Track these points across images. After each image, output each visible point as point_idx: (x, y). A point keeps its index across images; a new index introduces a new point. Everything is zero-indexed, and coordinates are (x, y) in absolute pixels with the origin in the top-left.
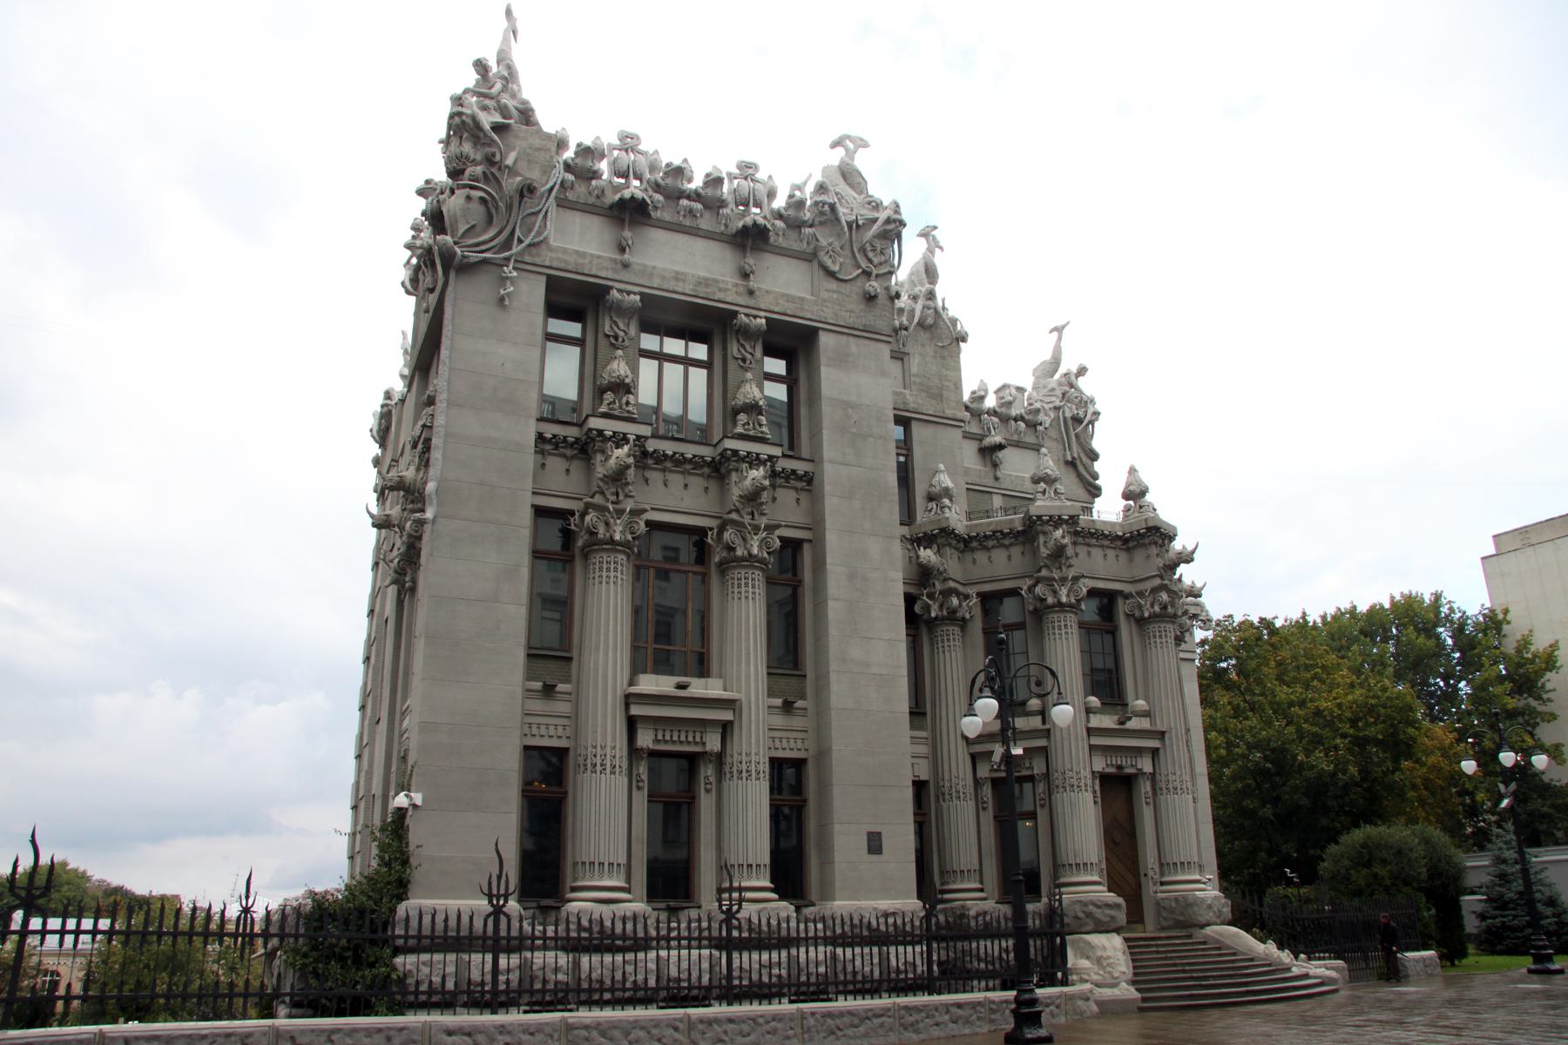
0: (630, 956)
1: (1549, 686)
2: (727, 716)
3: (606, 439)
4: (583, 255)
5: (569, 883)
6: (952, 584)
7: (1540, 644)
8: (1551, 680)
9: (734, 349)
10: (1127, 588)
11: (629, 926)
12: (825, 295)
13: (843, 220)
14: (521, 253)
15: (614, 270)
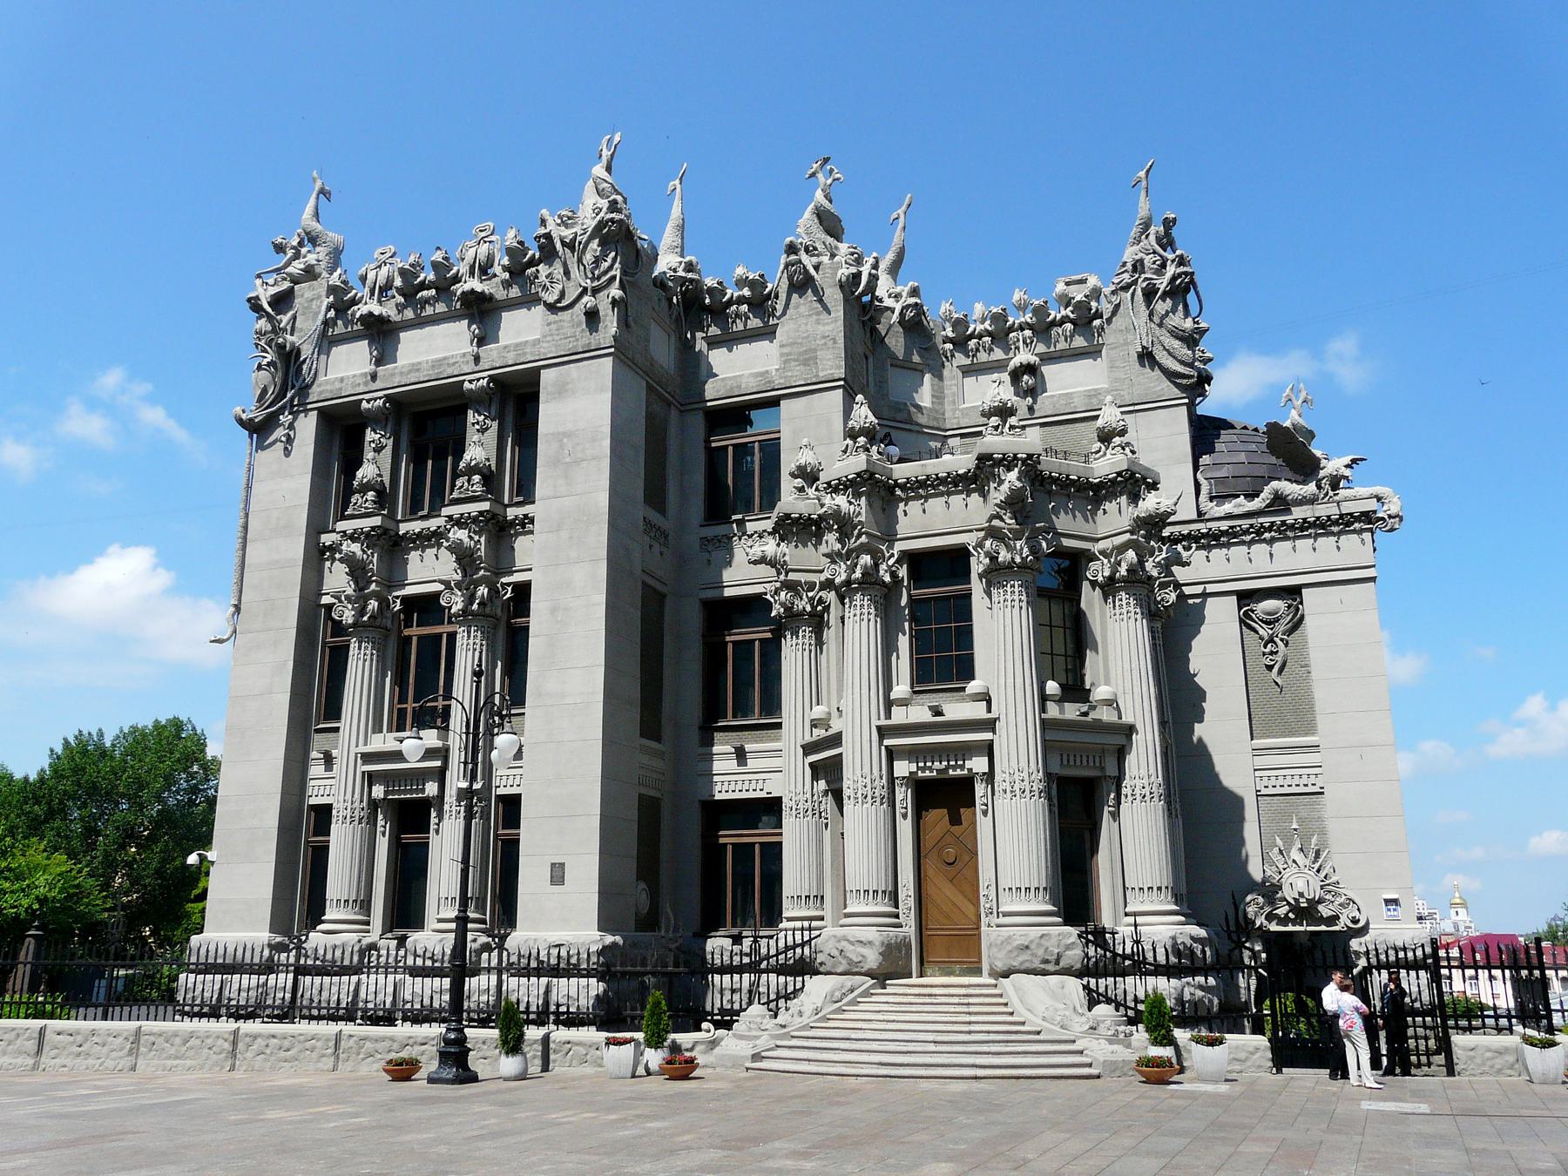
0: (336, 979)
2: (438, 763)
4: (342, 380)
6: (792, 576)
11: (338, 953)
13: (558, 246)
15: (366, 384)
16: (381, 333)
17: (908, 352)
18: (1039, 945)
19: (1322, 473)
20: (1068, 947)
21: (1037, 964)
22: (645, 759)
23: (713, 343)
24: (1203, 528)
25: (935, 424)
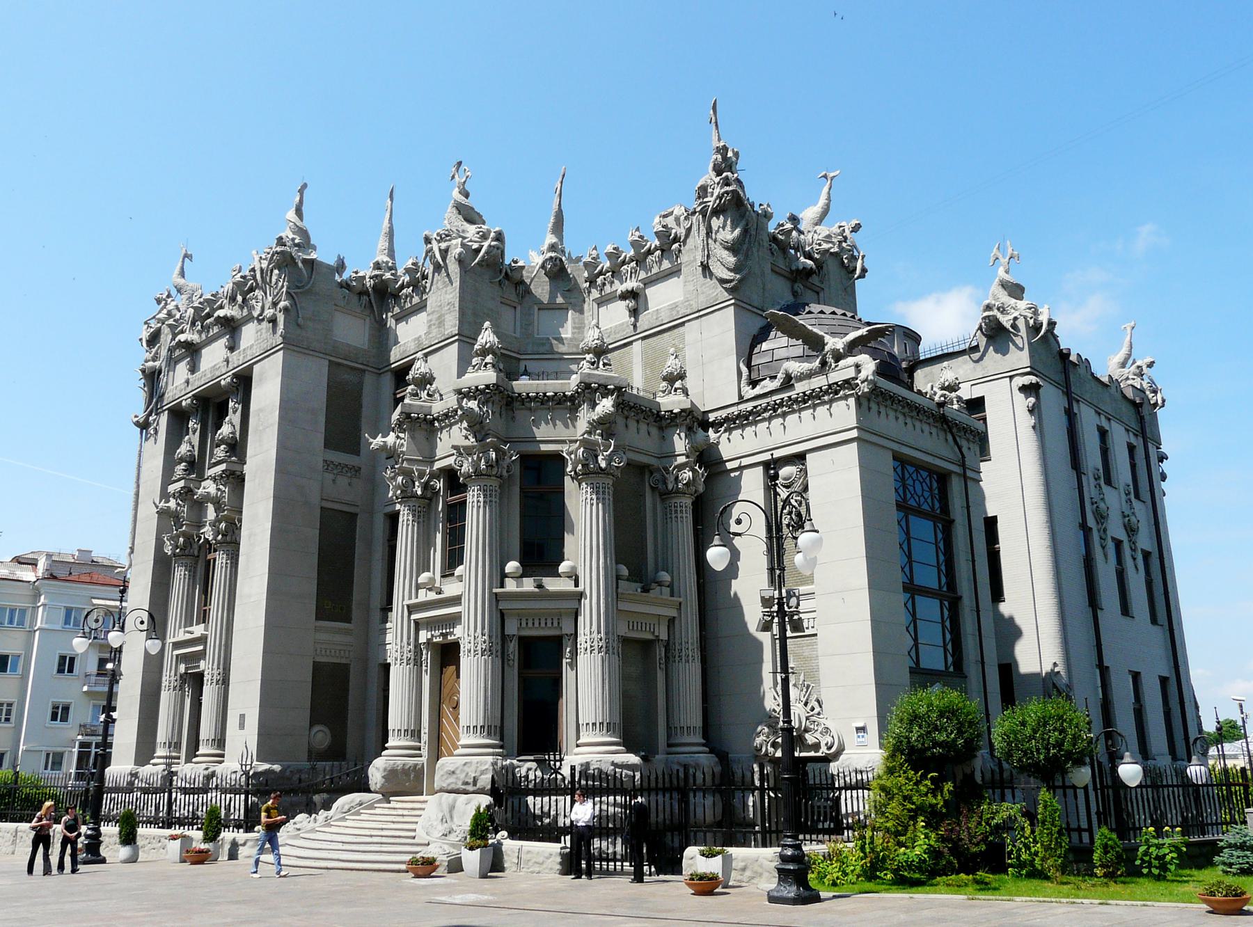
17: (553, 296)
18: (462, 771)
19: (827, 348)
20: (482, 773)
21: (460, 786)
22: (323, 636)
23: (398, 319)
24: (735, 410)
25: (574, 350)
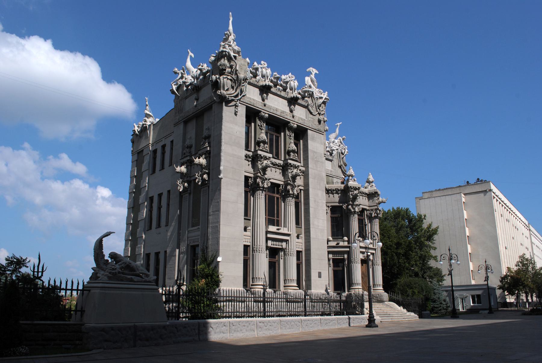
1: (434, 239)
3: (262, 158)
5: (251, 283)
7: (434, 226)
8: (435, 237)
9: (287, 133)
10: (368, 208)
12: (310, 119)
14: (241, 98)
16: (265, 90)
